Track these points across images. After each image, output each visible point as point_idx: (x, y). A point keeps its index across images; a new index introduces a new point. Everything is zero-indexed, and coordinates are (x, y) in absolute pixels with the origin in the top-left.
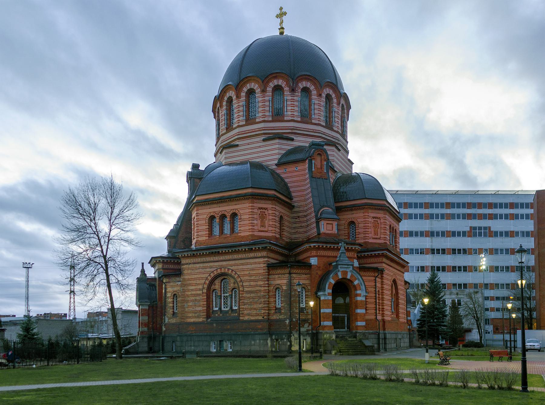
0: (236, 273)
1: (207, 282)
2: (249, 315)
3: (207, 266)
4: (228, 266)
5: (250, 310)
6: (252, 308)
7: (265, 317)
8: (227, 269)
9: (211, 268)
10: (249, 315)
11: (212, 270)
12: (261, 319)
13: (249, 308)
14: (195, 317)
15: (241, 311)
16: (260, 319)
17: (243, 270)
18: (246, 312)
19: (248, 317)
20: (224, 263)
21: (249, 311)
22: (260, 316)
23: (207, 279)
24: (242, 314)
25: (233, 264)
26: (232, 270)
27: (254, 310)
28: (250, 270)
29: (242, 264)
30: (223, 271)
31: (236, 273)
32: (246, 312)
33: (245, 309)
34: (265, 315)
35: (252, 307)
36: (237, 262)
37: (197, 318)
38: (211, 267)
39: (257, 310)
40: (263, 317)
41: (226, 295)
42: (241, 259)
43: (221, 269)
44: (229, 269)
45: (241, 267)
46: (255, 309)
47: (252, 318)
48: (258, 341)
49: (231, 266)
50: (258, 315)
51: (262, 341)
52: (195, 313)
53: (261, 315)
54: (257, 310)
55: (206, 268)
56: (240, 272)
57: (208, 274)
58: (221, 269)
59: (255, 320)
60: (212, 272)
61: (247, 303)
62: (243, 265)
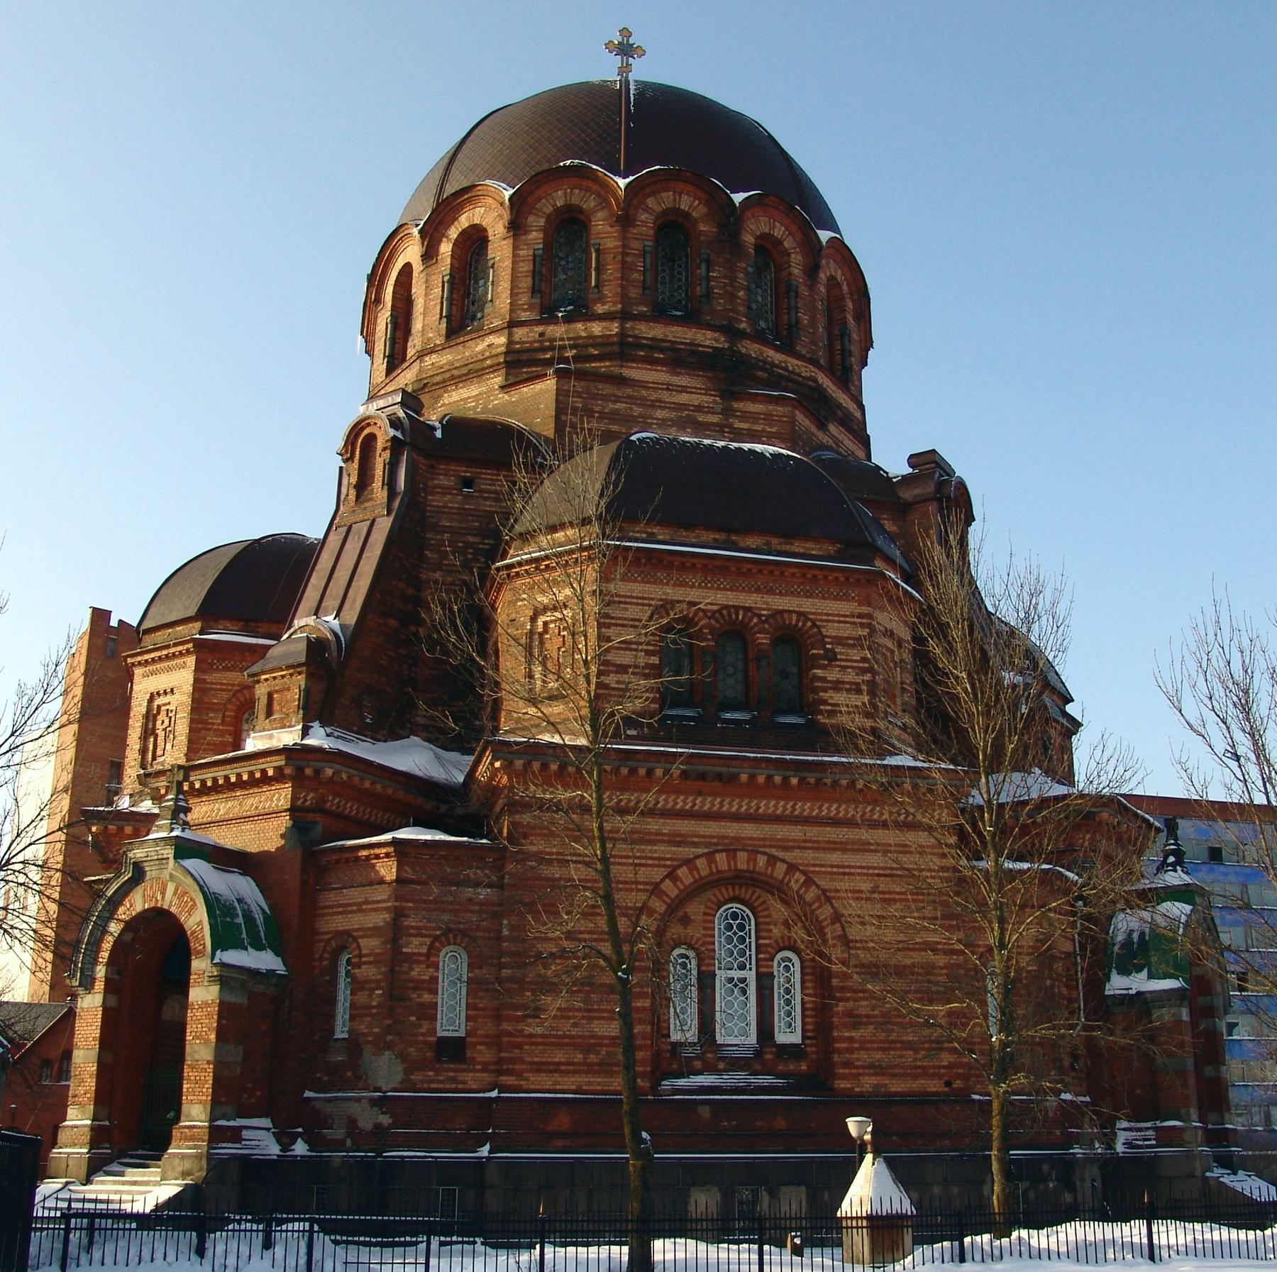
0: (809, 882)
1: (660, 907)
2: (877, 1069)
3: (657, 834)
4: (772, 847)
5: (883, 1049)
6: (893, 1042)
7: (958, 1084)
8: (762, 861)
9: (678, 844)
10: (877, 1069)
11: (689, 852)
12: (937, 1094)
13: (880, 1042)
14: (589, 1069)
15: (840, 1052)
16: (932, 1094)
17: (845, 872)
18: (862, 1057)
19: (874, 1080)
20: (748, 830)
21: (879, 1055)
22: (933, 1076)
23: (656, 889)
24: (848, 1064)
25: (794, 841)
26: (792, 868)
27: (904, 1049)
28: (879, 875)
29: (842, 847)
30: (742, 865)
31: (809, 882)
32: (862, 1057)
33: (860, 1042)
34: (958, 1076)
35: (893, 1037)
36: (812, 832)
37: (599, 1073)
38: (677, 840)
39: (916, 1050)
40: (948, 1084)
41: (737, 974)
42: (836, 822)
43: (731, 853)
44: (773, 860)
45: (835, 858)
46: (908, 1046)
47: (897, 1086)
48: (936, 1190)
49: (787, 849)
50: (925, 1073)
51: (955, 1190)
52: (587, 1049)
53: (940, 1076)
54: (916, 1050)
55: (651, 842)
56: (831, 880)
57: (665, 872)
58: (731, 853)
59: (912, 1094)
60: (689, 862)
61: (867, 1016)
62: (844, 851)
